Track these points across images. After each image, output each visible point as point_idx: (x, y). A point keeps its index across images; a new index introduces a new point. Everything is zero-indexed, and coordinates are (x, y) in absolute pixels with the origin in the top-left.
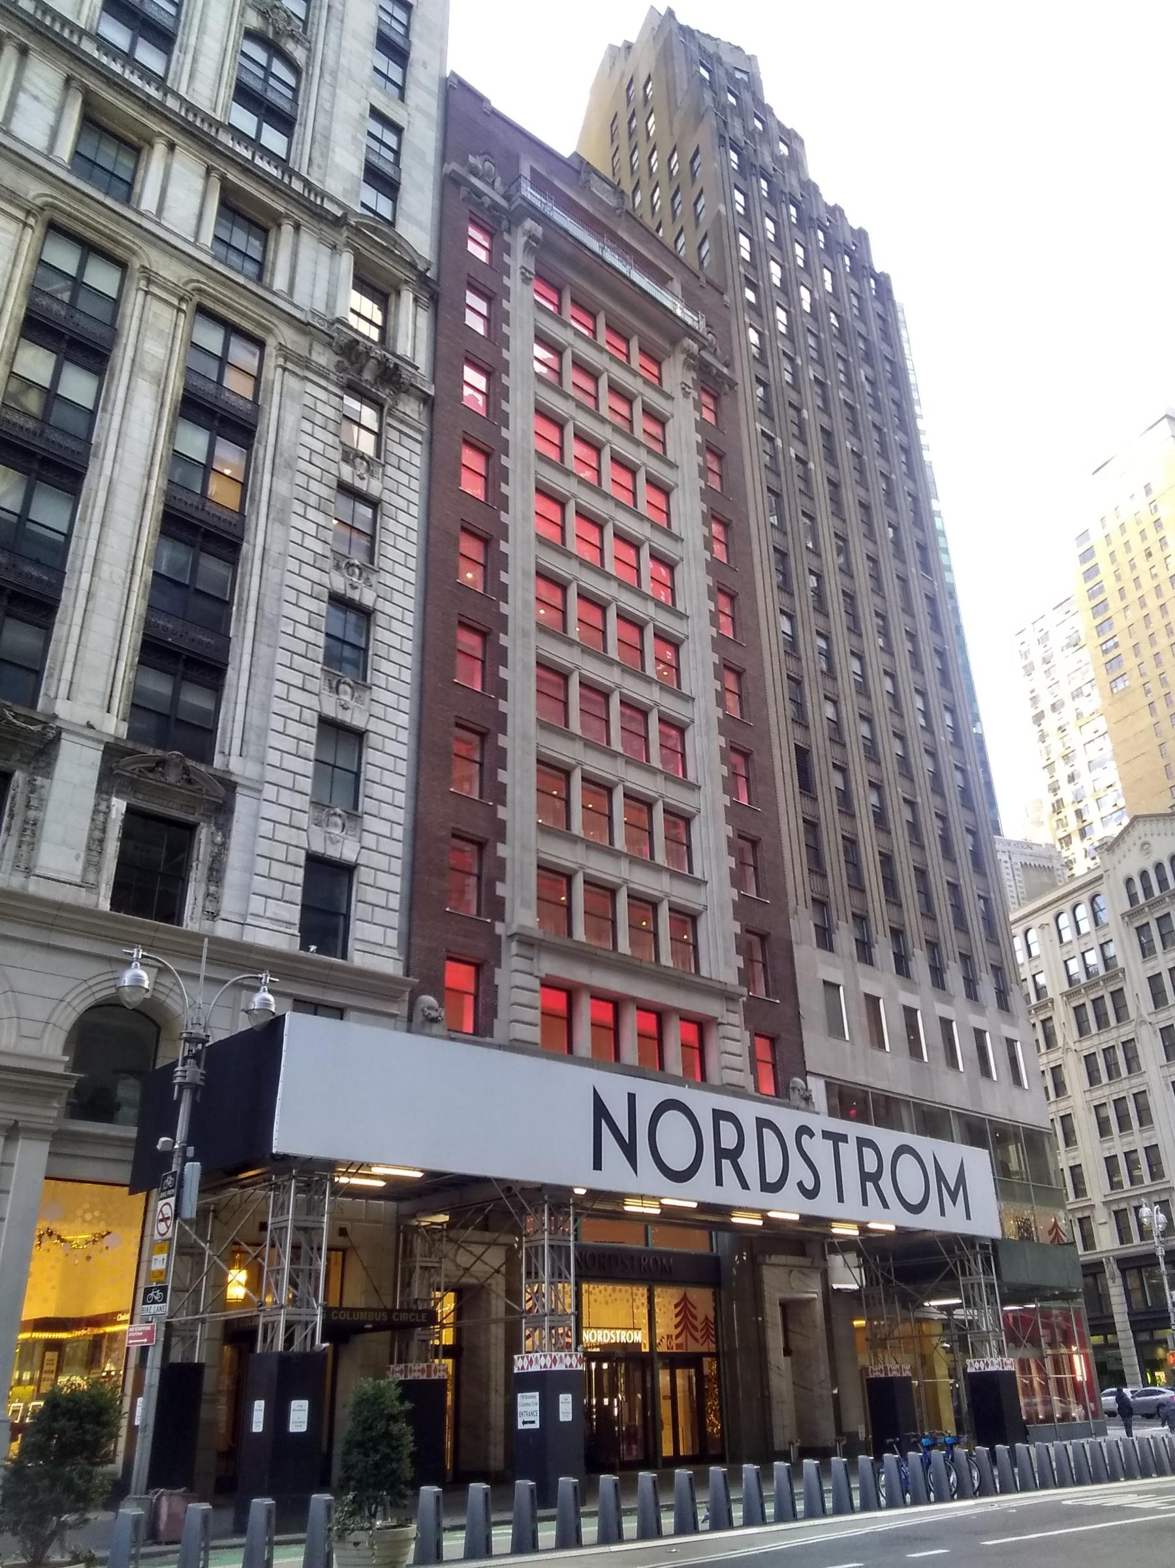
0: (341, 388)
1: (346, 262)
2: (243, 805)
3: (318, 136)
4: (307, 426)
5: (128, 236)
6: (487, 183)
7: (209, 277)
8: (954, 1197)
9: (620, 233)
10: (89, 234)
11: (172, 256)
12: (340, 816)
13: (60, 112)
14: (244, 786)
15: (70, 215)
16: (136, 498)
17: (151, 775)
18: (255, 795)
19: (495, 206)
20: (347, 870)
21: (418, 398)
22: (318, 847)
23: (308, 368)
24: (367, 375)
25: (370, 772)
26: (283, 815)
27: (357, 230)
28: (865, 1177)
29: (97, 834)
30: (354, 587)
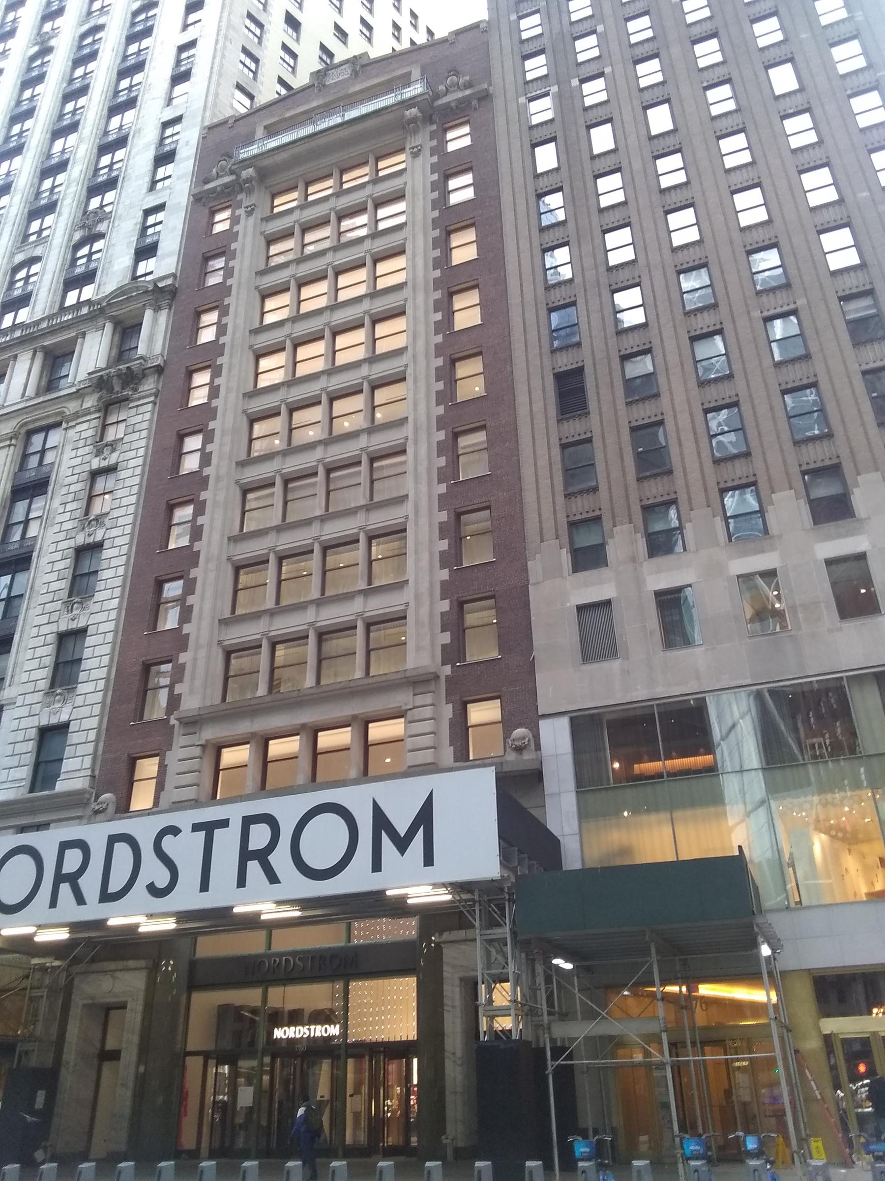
0: (99, 411)
1: (109, 327)
4: (74, 453)
6: (222, 176)
7: (27, 413)
8: (402, 844)
18: (12, 706)
19: (226, 186)
20: (63, 728)
22: (44, 722)
23: (78, 417)
24: (117, 388)
25: (87, 653)
26: (24, 711)
27: (109, 305)
28: (246, 855)
30: (89, 535)
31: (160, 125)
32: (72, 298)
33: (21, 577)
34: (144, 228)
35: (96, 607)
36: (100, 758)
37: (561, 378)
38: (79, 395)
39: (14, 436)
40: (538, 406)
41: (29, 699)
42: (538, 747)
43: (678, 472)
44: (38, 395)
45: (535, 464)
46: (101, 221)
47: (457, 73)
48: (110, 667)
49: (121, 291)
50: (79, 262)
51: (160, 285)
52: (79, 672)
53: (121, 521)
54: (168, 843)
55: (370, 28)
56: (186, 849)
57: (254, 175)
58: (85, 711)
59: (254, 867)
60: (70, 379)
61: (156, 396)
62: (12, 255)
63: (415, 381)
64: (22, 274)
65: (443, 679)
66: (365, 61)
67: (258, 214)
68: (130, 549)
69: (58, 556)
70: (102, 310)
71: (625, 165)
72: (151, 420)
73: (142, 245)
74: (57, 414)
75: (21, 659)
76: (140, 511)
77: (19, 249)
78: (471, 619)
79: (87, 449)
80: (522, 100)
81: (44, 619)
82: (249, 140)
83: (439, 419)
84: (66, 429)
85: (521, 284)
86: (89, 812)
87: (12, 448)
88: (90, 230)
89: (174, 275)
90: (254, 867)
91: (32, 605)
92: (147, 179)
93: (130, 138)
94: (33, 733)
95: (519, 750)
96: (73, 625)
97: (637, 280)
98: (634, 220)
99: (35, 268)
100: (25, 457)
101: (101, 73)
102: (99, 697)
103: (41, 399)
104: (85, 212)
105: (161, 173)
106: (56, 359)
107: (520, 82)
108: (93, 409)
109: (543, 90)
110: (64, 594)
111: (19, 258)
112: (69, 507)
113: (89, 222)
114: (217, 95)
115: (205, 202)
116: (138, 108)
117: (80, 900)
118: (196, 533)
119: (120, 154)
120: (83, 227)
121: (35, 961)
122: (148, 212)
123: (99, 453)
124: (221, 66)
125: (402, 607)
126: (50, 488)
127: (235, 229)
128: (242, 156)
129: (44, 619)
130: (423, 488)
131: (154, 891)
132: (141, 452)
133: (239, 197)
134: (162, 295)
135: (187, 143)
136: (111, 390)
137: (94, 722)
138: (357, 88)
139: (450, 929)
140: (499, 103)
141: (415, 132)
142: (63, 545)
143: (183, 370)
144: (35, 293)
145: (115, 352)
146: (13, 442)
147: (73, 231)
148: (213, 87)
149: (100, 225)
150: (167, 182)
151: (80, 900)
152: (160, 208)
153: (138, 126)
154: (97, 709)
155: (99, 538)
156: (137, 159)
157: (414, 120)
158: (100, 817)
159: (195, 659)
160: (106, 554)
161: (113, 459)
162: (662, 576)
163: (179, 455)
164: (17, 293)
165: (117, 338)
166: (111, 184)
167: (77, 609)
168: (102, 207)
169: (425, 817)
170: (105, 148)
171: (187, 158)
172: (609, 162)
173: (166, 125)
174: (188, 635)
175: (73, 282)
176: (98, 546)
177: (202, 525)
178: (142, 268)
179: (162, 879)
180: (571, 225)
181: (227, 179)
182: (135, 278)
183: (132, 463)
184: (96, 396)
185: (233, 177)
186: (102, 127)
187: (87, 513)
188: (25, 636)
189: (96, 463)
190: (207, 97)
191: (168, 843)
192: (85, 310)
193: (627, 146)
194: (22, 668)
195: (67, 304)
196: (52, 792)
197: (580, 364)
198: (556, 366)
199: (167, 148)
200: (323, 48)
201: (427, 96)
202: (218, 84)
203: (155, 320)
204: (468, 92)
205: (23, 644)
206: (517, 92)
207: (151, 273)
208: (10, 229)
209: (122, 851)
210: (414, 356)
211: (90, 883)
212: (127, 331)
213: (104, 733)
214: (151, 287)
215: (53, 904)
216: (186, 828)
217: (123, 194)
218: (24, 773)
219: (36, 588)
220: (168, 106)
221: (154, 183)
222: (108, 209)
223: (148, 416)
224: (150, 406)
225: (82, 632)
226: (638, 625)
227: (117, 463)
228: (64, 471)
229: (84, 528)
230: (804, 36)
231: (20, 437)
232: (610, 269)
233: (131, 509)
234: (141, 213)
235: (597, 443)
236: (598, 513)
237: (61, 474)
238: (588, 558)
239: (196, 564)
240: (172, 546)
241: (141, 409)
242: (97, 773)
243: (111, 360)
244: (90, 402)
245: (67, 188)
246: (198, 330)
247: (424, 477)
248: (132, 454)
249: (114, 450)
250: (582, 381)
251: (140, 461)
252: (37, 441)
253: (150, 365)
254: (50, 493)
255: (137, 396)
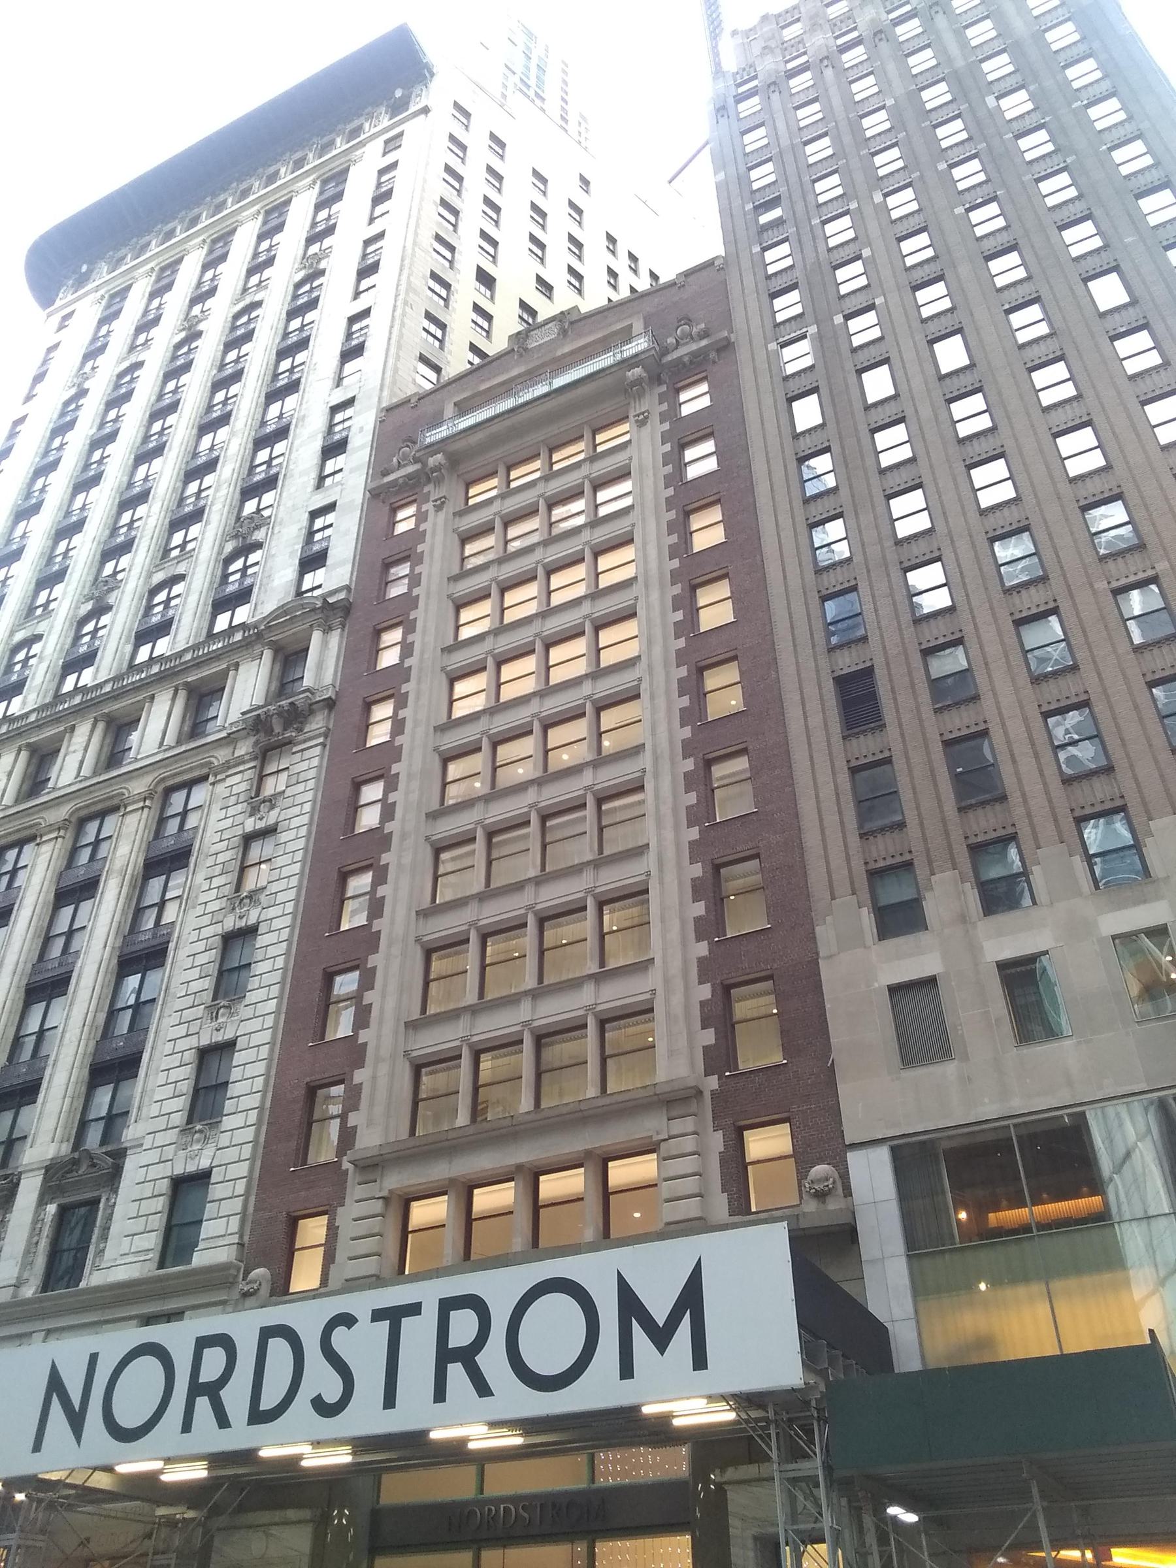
0: (255, 758)
1: (268, 654)
2: (131, 1164)
3: (265, 581)
5: (115, 789)
6: (405, 466)
7: (166, 766)
8: (661, 1337)
9: (559, 353)
10: (99, 807)
11: (143, 775)
12: (200, 1131)
13: (86, 749)
14: (131, 1148)
15: (87, 806)
16: (96, 966)
17: (68, 1176)
18: (139, 1150)
19: (409, 477)
21: (322, 709)
22: (179, 1170)
23: (229, 768)
24: (277, 729)
25: (236, 1074)
26: (153, 1156)
27: (268, 628)
28: (445, 1355)
29: (35, 1239)
30: (241, 918)
31: (328, 410)
32: (222, 622)
33: (154, 977)
34: (311, 533)
35: (248, 1012)
36: (250, 1219)
37: (843, 682)
38: (230, 740)
39: (149, 796)
40: (816, 720)
41: (161, 1139)
42: (848, 1191)
43: (1015, 797)
44: (179, 742)
45: (817, 796)
46: (258, 527)
47: (689, 322)
48: (264, 1092)
49: (282, 610)
50: (231, 579)
51: (330, 600)
52: (224, 1099)
53: (281, 898)
54: (340, 1337)
55: (579, 277)
56: (364, 1346)
57: (443, 462)
58: (231, 1154)
59: (456, 1371)
60: (219, 722)
61: (326, 735)
62: (150, 575)
63: (652, 697)
64: (162, 596)
65: (707, 1096)
66: (575, 317)
67: (449, 508)
68: (291, 934)
69: (201, 946)
70: (259, 635)
71: (909, 413)
72: (319, 767)
73: (309, 553)
74: (202, 766)
75: (150, 1086)
76: (305, 882)
77: (158, 567)
78: (741, 1009)
79: (240, 808)
80: (773, 346)
81: (182, 1030)
82: (436, 421)
83: (686, 743)
84: (213, 784)
85: (784, 570)
86: (235, 1295)
87: (146, 810)
88: (244, 541)
89: (347, 588)
90: (456, 1371)
91: (167, 1012)
92: (314, 475)
93: (292, 427)
94: (164, 1186)
95: (821, 1196)
96: (219, 1037)
97: (936, 554)
98: (927, 480)
99: (177, 589)
100: (162, 821)
101: (258, 356)
102: (249, 1134)
103: (183, 748)
104: (238, 518)
105: (330, 466)
106: (202, 697)
107: (769, 325)
108: (247, 757)
109: (799, 332)
110: (207, 997)
111: (159, 577)
112: (216, 882)
113: (243, 530)
114: (396, 370)
115: (384, 498)
116: (301, 392)
117: (223, 1421)
118: (376, 908)
119: (280, 448)
120: (236, 537)
121: (162, 1511)
122: (314, 515)
123: (254, 811)
124: (401, 336)
125: (648, 996)
126: (192, 860)
127: (422, 527)
128: (428, 440)
129: (182, 1030)
130: (669, 835)
131: (323, 1408)
132: (307, 807)
133: (426, 490)
134: (332, 612)
135: (361, 429)
136: (270, 731)
137: (243, 1169)
138: (567, 349)
139: (736, 1462)
140: (743, 354)
141: (640, 395)
142: (207, 932)
143: (360, 702)
144: (176, 618)
145: (275, 685)
146: (148, 803)
147: (224, 541)
148: (391, 361)
149: (256, 532)
150: (338, 477)
151: (223, 1421)
152: (331, 507)
153: (302, 413)
154: (247, 1151)
155: (252, 920)
156: (301, 452)
157: (638, 382)
158: (250, 1301)
159: (374, 1077)
160: (261, 941)
161: (272, 817)
162: (1006, 940)
163: (355, 808)
164: (155, 620)
165: (277, 667)
166: (270, 483)
167: (223, 1015)
168: (259, 511)
169: (691, 1298)
170: (262, 442)
171: (362, 447)
172: (891, 411)
173: (335, 410)
174: (365, 1044)
175: (224, 603)
176: (251, 932)
177: (384, 897)
178: (309, 581)
179: (332, 1391)
180: (844, 492)
181: (411, 469)
182: (299, 593)
183: (295, 822)
184: (252, 740)
185: (418, 466)
186: (259, 416)
187: (238, 888)
188: (157, 1053)
189: (250, 825)
190: (384, 373)
191: (340, 1337)
192: (238, 637)
193: (910, 390)
194: (152, 1097)
195: (217, 630)
196: (188, 1267)
197: (868, 664)
198: (835, 668)
199: (337, 437)
200: (523, 305)
201: (653, 352)
202: (398, 358)
203: (325, 644)
204: (704, 343)
205: (153, 1066)
206: (765, 338)
207: (320, 586)
208: (147, 544)
209: (279, 1348)
210: (650, 667)
211: (236, 1397)
212: (290, 658)
213: (255, 1182)
214: (319, 604)
215: (187, 1427)
216: (363, 1316)
217: (284, 495)
218: (152, 1241)
219: (172, 990)
220: (338, 386)
221: (321, 479)
222: (266, 513)
223: (315, 762)
224: (318, 750)
225: (229, 1046)
226: (976, 1012)
227: (277, 823)
228: (211, 836)
229: (234, 909)
230: (1128, 240)
231: (156, 796)
232: (899, 543)
233: (294, 881)
234: (307, 515)
235: (899, 764)
236: (907, 857)
237: (206, 840)
238: (899, 919)
239: (375, 949)
240: (345, 926)
241: (307, 754)
242: (246, 1239)
243: (270, 694)
244: (244, 748)
245: (217, 490)
246: (377, 652)
247: (669, 821)
248: (296, 810)
249: (272, 808)
250: (873, 685)
251: (305, 819)
252: (178, 799)
253: (318, 699)
254: (192, 865)
255: (301, 738)
